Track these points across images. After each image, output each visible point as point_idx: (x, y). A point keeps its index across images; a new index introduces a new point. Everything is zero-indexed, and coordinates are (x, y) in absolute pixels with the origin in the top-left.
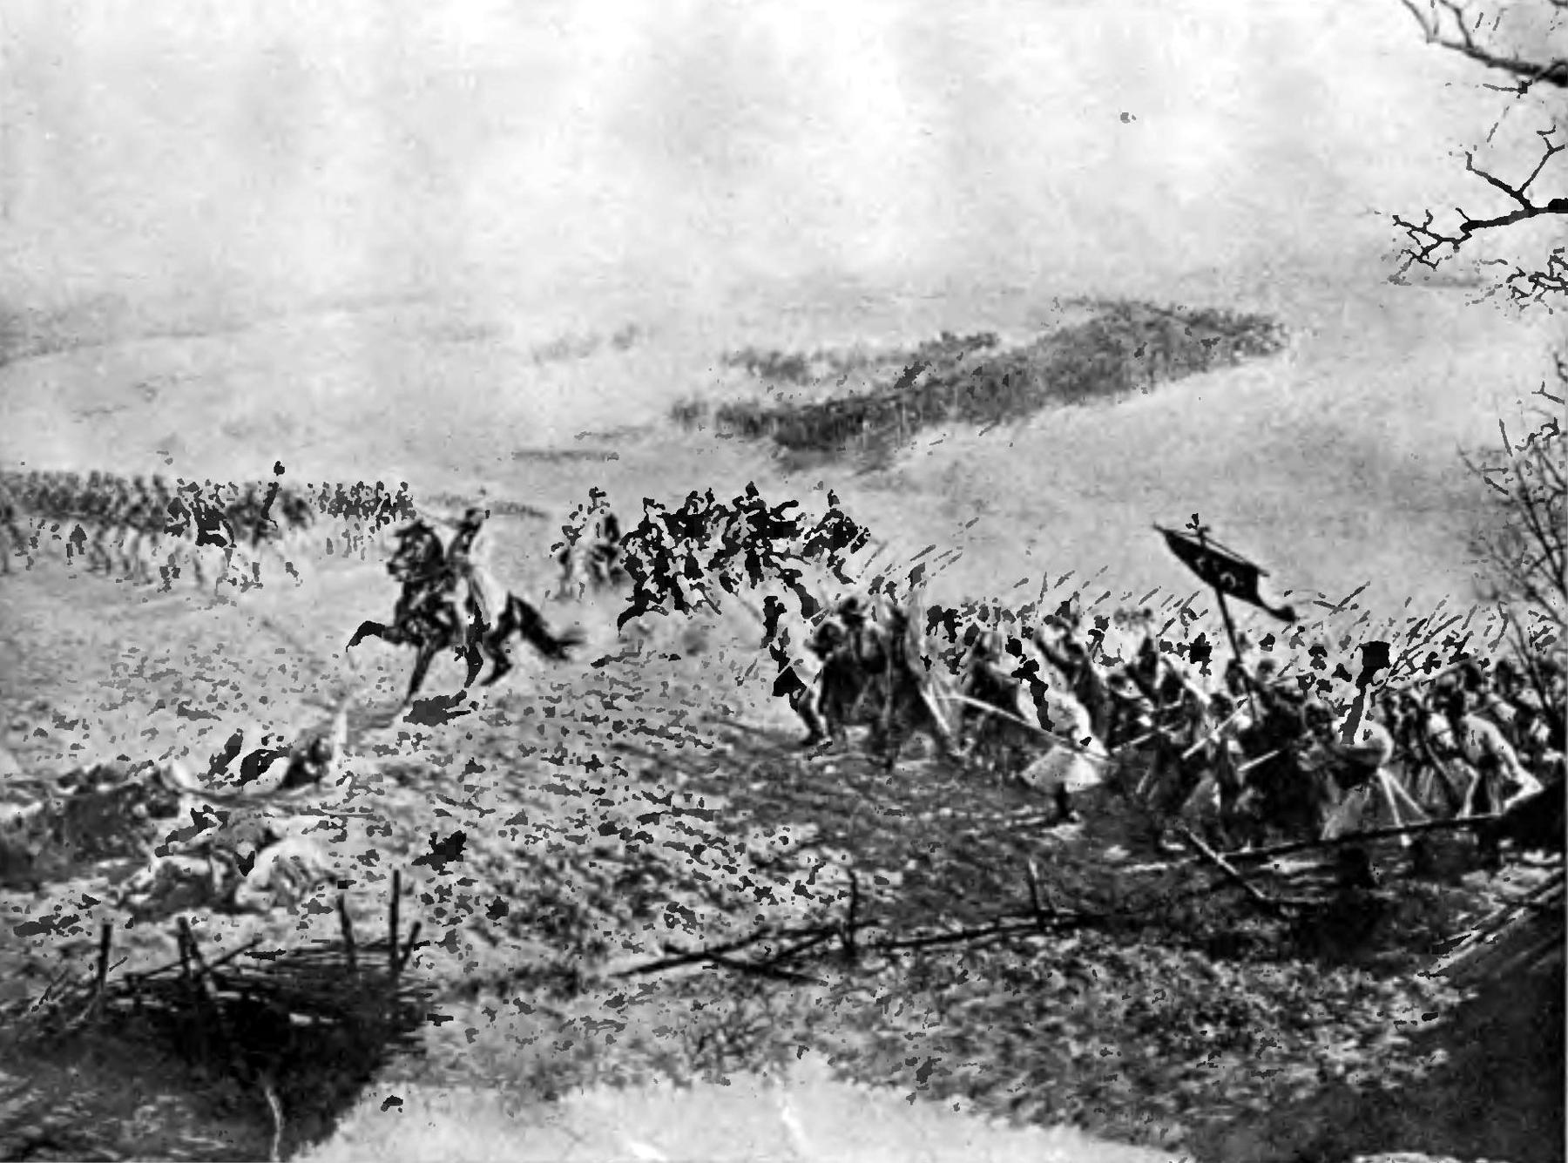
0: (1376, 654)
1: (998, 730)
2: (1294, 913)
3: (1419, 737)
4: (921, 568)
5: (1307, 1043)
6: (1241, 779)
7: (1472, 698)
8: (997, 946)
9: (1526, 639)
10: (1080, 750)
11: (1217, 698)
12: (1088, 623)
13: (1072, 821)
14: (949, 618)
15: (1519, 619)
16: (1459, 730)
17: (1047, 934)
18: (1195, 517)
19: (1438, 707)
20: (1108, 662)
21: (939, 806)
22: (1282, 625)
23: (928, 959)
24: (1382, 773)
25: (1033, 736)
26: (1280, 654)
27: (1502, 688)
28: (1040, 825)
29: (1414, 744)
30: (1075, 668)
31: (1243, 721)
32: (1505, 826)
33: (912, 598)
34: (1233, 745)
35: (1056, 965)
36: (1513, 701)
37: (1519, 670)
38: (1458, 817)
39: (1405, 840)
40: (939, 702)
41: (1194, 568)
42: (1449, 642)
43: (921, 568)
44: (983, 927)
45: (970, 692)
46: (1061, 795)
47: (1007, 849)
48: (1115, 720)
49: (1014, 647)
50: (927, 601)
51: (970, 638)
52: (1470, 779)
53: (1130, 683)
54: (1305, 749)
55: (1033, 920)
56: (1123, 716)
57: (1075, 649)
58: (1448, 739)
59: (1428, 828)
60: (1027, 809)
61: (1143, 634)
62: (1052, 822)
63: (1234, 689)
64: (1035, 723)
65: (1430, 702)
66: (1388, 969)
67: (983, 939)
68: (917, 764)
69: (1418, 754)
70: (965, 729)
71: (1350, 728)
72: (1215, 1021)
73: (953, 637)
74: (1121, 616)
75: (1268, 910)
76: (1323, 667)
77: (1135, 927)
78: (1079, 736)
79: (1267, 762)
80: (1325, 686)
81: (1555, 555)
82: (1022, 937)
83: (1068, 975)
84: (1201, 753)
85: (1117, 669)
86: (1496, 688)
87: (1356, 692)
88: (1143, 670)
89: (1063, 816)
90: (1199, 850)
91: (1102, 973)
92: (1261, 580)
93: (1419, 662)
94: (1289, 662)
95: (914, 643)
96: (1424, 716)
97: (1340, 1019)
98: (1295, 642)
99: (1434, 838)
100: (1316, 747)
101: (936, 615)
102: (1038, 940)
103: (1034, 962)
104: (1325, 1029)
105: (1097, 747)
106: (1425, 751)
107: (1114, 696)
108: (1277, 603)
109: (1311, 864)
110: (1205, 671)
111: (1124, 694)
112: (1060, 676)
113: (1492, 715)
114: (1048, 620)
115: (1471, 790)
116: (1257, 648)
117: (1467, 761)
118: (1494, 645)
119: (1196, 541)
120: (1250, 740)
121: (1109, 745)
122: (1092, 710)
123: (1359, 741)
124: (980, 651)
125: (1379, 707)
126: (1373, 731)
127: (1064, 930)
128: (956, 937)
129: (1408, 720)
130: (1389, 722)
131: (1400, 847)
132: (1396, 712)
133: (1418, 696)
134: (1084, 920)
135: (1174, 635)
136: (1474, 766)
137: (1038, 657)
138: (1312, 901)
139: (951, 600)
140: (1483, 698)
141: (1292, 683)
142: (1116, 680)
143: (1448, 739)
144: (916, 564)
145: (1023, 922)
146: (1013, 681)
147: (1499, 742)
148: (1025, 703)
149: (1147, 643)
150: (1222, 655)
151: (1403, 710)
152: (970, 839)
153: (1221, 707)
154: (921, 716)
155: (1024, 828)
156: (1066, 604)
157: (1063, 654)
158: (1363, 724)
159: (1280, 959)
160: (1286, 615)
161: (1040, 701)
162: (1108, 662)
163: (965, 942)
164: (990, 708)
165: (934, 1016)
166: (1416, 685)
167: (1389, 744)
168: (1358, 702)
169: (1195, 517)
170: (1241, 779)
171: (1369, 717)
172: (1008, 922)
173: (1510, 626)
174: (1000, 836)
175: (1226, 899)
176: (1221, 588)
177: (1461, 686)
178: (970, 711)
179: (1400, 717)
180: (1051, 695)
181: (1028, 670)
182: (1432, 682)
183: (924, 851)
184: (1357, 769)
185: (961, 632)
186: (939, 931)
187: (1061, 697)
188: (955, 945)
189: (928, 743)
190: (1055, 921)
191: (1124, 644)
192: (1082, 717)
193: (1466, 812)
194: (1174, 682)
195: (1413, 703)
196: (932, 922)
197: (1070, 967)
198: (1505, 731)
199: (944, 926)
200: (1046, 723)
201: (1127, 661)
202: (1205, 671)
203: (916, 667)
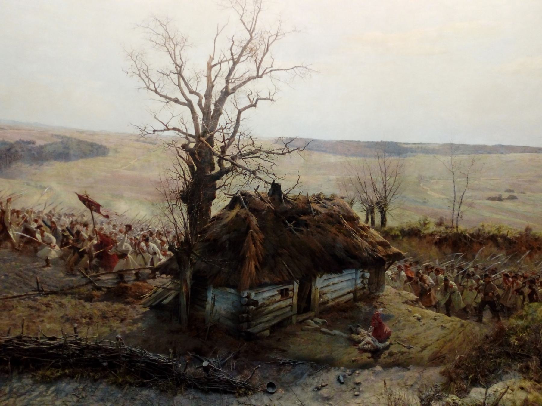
0: (129, 227)
1: (30, 242)
2: (105, 290)
3: (138, 247)
4: (10, 199)
5: (107, 322)
6: (94, 256)
7: (151, 238)
8: (27, 299)
9: (164, 225)
10: (53, 248)
11: (90, 236)
12: (57, 216)
13: (50, 266)
14: (18, 212)
15: (162, 220)
16: (147, 246)
17: (41, 296)
18: (86, 192)
19: (143, 240)
20: (62, 226)
21: (11, 262)
22: (106, 219)
23: (6, 303)
24: (129, 255)
25: (40, 244)
26: (105, 226)
27: (158, 236)
28: (40, 268)
29: (137, 249)
30: (53, 229)
31: (95, 242)
32: (157, 269)
33: (7, 206)
34: (92, 248)
35: (43, 304)
36: (160, 240)
37: (162, 233)
38: (147, 267)
39: (134, 272)
40: (13, 234)
41: (85, 204)
42: (146, 225)
43: (10, 199)
44: (23, 294)
45: (23, 232)
46: (47, 260)
47: (31, 274)
48: (62, 241)
49: (36, 221)
50: (11, 208)
51: (23, 218)
52: (150, 257)
53: (67, 231)
54: (110, 249)
55: (38, 292)
56: (65, 240)
57: (53, 223)
58: (145, 248)
59: (139, 269)
60: (37, 263)
61: (71, 219)
62: (44, 267)
63: (94, 234)
64: (40, 240)
65: (141, 239)
66: (127, 303)
67: (23, 297)
68: (6, 250)
69: (138, 251)
70: (20, 241)
71: (122, 245)
72: (85, 318)
73: (18, 217)
74: (66, 215)
75: (99, 289)
76: (116, 230)
77: (66, 294)
78: (52, 245)
79: (102, 252)
80: (116, 234)
81: (171, 206)
82: (34, 297)
83: (47, 307)
84: (84, 250)
85: (64, 228)
86: (156, 237)
87: (123, 236)
88: (70, 230)
89: (48, 265)
90: (83, 274)
91: (56, 306)
92: (101, 208)
93: (139, 229)
94: (107, 229)
95: (7, 218)
96: (140, 242)
97: (115, 316)
98: (109, 223)
99: (141, 271)
100: (113, 249)
101: (13, 211)
102: (39, 298)
103: (37, 303)
104: (112, 318)
105: (57, 247)
106: (139, 251)
107: (63, 235)
108: (105, 214)
109: (110, 277)
110: (87, 230)
111: (65, 234)
112: (49, 229)
113: (155, 242)
114: (46, 214)
115: (150, 260)
116: (99, 225)
117: (149, 253)
118: (156, 226)
119: (86, 198)
120: (97, 247)
121: (61, 246)
122: (57, 238)
123: (124, 248)
124: (26, 221)
125: (129, 240)
126: (127, 246)
127: (47, 294)
128: (15, 297)
129: (136, 243)
130: (131, 244)
131: (132, 274)
132: (133, 241)
133: (138, 237)
134: (53, 293)
135: (79, 219)
136: (151, 255)
137: (43, 224)
138: (110, 286)
139: (18, 208)
140: (153, 239)
141: (108, 233)
142: (63, 231)
143: (145, 248)
144: (9, 197)
145: (35, 293)
146: (35, 229)
147: (157, 249)
148: (38, 236)
149: (72, 222)
150: (91, 226)
151: (134, 241)
152: (20, 271)
153: (91, 239)
154: (8, 237)
155: (35, 268)
156: (50, 212)
157: (49, 223)
158: (125, 244)
159: (102, 301)
160: (107, 217)
161: (42, 235)
162: (62, 226)
163: (18, 298)
164: (28, 236)
165: (7, 318)
166: (138, 235)
167: (131, 248)
168: (124, 238)
169: (86, 192)
170: (94, 256)
171: (126, 242)
172: (30, 293)
173: (160, 222)
174: (30, 270)
175: (90, 287)
176: (91, 210)
177: (149, 235)
178: (22, 237)
179: (134, 242)
180: (46, 233)
181: (39, 227)
182: (142, 235)
183: (7, 274)
184: (124, 255)
185: (21, 216)
186: (10, 295)
187: (48, 234)
188: (14, 299)
189: (9, 245)
190: (44, 293)
191: (66, 221)
192: (54, 240)
193: (149, 265)
194: (78, 232)
195: (137, 239)
196: (8, 293)
197: (48, 305)
198: (158, 247)
199: (11, 294)
200: (43, 241)
201: (67, 226)
202: (87, 230)
203: (7, 225)
